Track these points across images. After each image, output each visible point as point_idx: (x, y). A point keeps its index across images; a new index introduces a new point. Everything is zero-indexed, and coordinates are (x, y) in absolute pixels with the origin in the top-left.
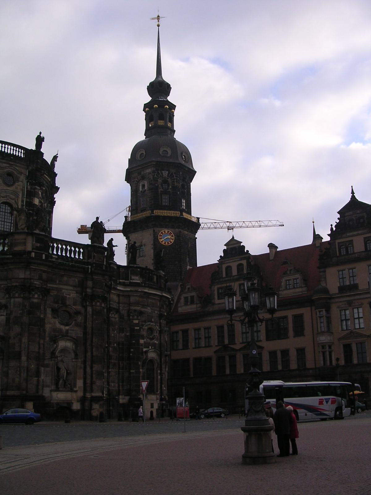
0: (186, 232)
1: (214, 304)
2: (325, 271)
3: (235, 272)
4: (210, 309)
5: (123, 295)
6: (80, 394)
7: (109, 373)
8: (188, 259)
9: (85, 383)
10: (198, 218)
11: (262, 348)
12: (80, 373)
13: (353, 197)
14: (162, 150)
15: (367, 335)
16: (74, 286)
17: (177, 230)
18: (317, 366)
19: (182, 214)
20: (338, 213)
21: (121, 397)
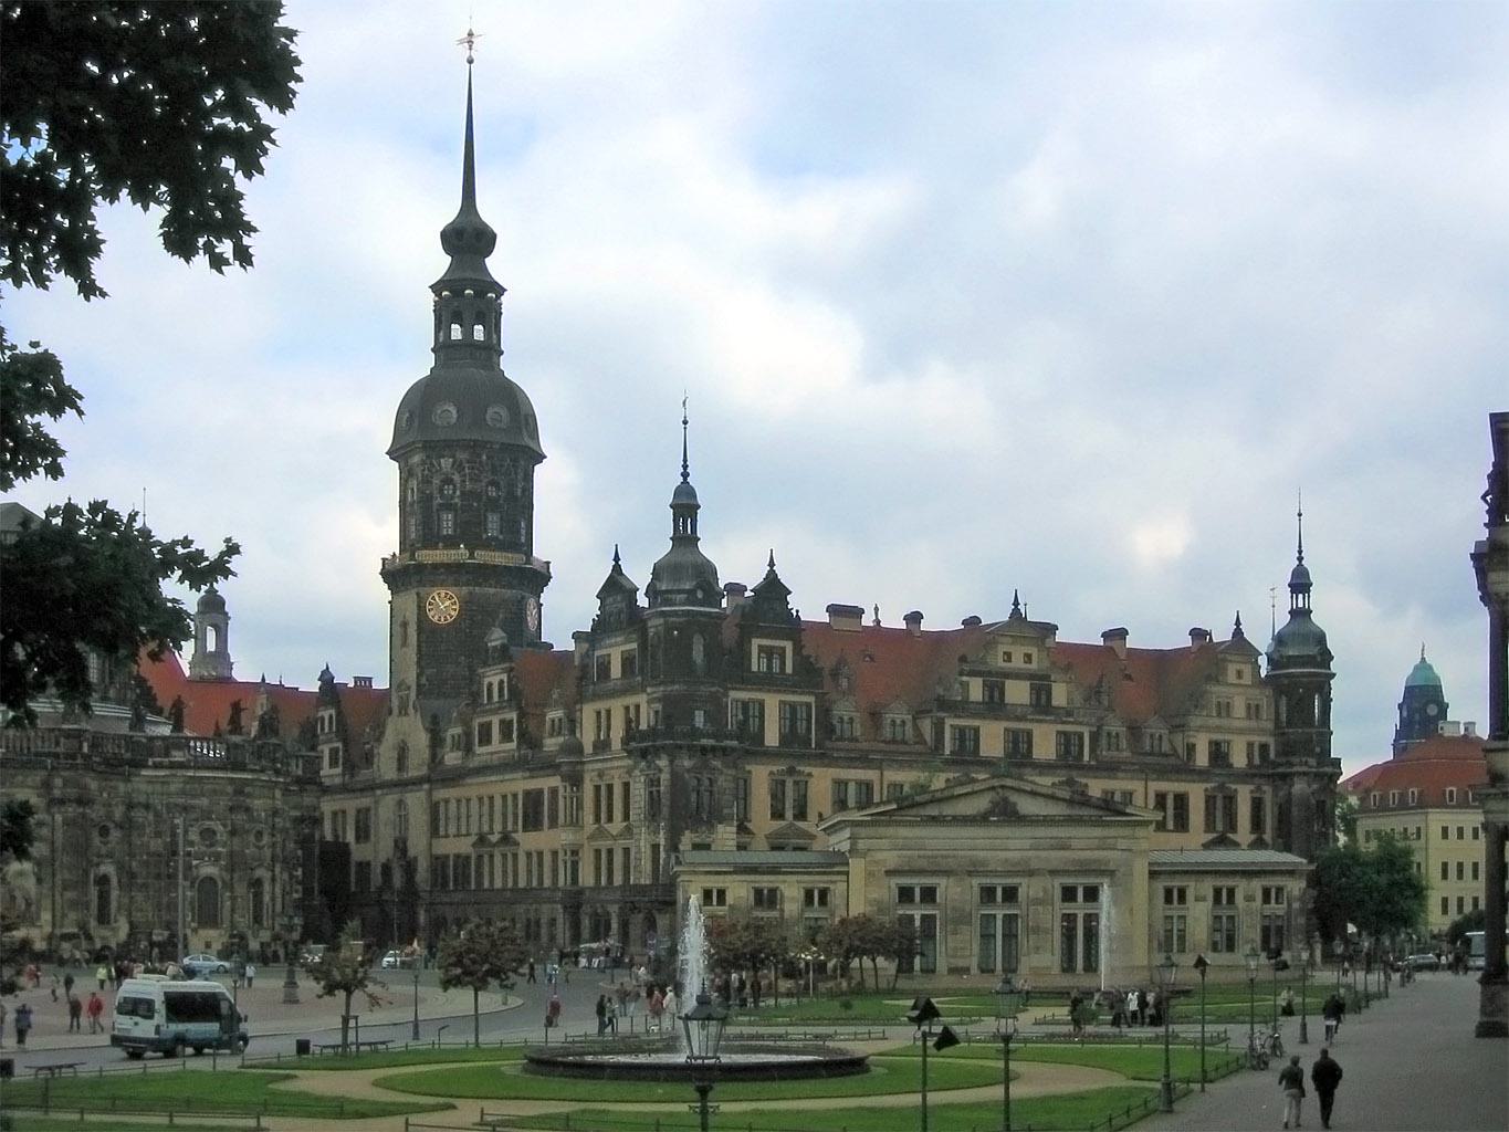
0: (492, 590)
1: (474, 753)
2: (581, 710)
3: (496, 698)
4: (474, 763)
6: (48, 929)
9: (54, 916)
12: (47, 903)
13: (617, 569)
15: (614, 834)
17: (465, 590)
19: (472, 556)
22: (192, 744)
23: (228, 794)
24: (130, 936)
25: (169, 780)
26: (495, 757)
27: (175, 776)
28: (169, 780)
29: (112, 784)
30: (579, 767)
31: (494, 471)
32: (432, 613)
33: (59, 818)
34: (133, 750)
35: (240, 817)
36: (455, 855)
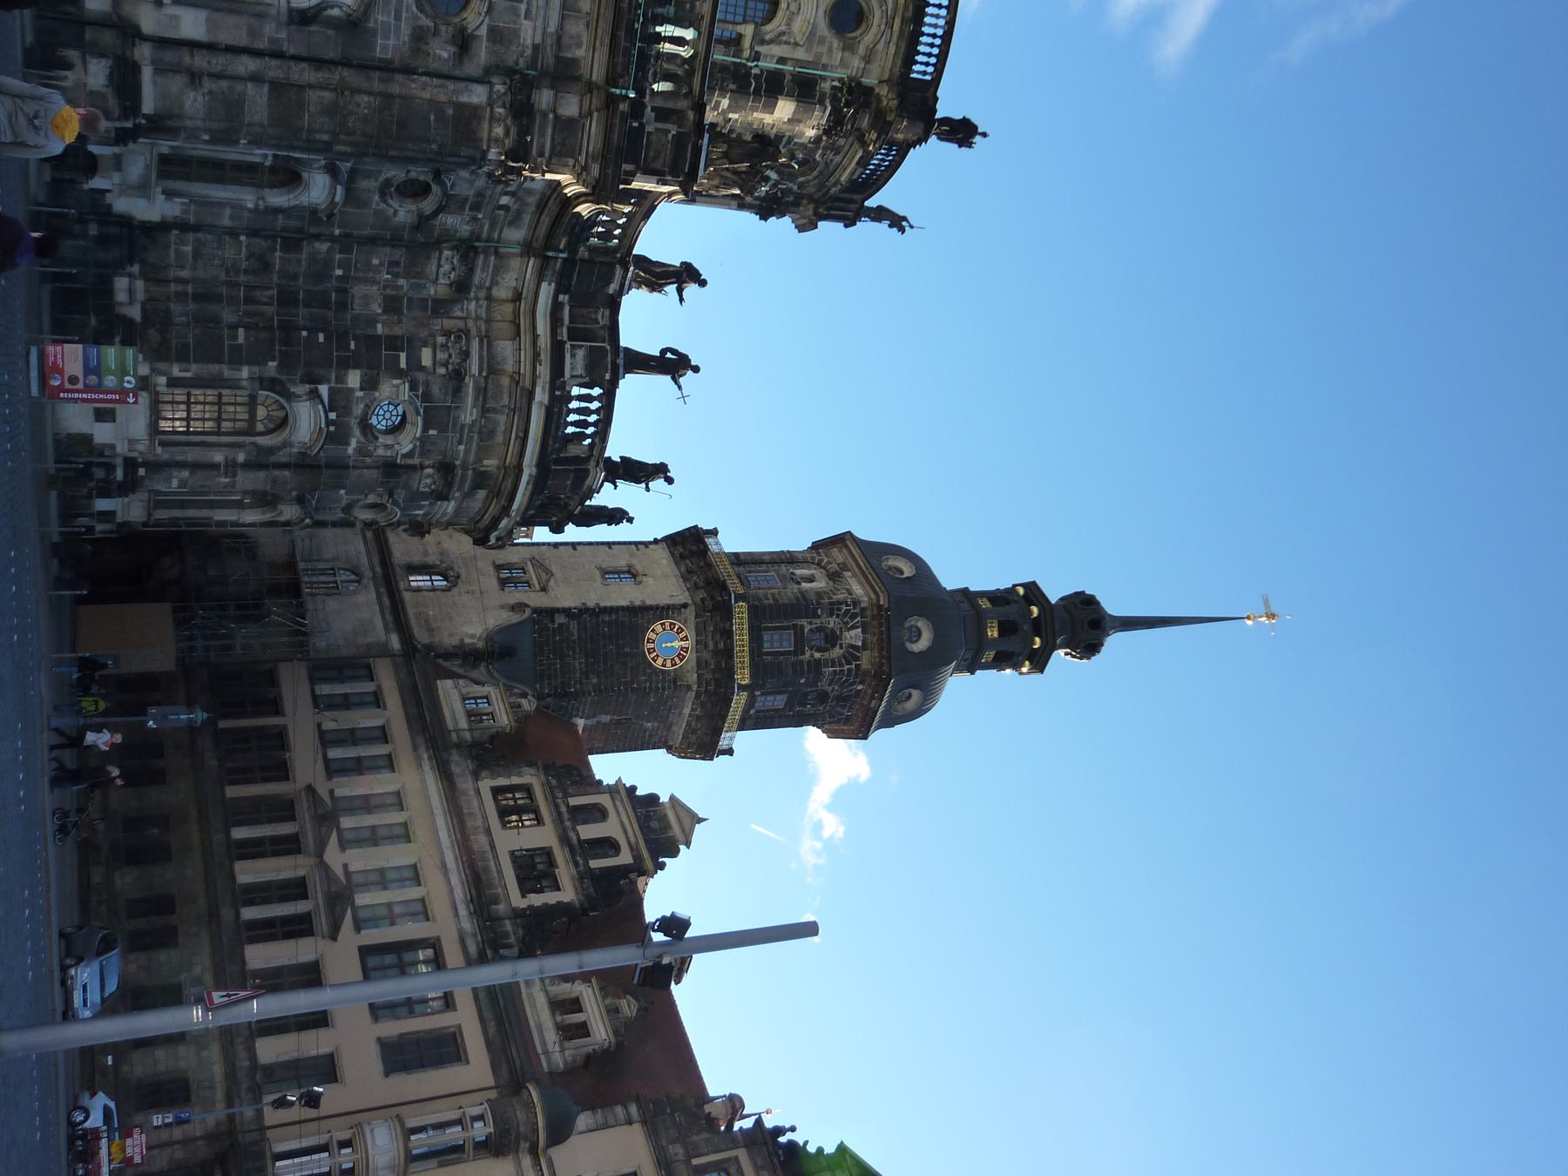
0: (687, 711)
1: (476, 776)
2: (630, 1122)
3: (588, 831)
5: (516, 313)
7: (233, 233)
8: (605, 718)
9: (193, 45)
10: (730, 752)
11: (334, 939)
12: (234, 31)
14: (922, 624)
16: (559, 39)
18: (270, 1134)
19: (742, 688)
20: (842, 1149)
21: (140, 284)
22: (597, 391)
23: (479, 460)
24: (126, 222)
25: (526, 339)
26: (483, 839)
27: (536, 356)
28: (526, 339)
29: (527, 218)
30: (525, 1145)
31: (841, 699)
32: (659, 628)
33: (477, 95)
34: (591, 262)
35: (426, 480)
36: (285, 727)
